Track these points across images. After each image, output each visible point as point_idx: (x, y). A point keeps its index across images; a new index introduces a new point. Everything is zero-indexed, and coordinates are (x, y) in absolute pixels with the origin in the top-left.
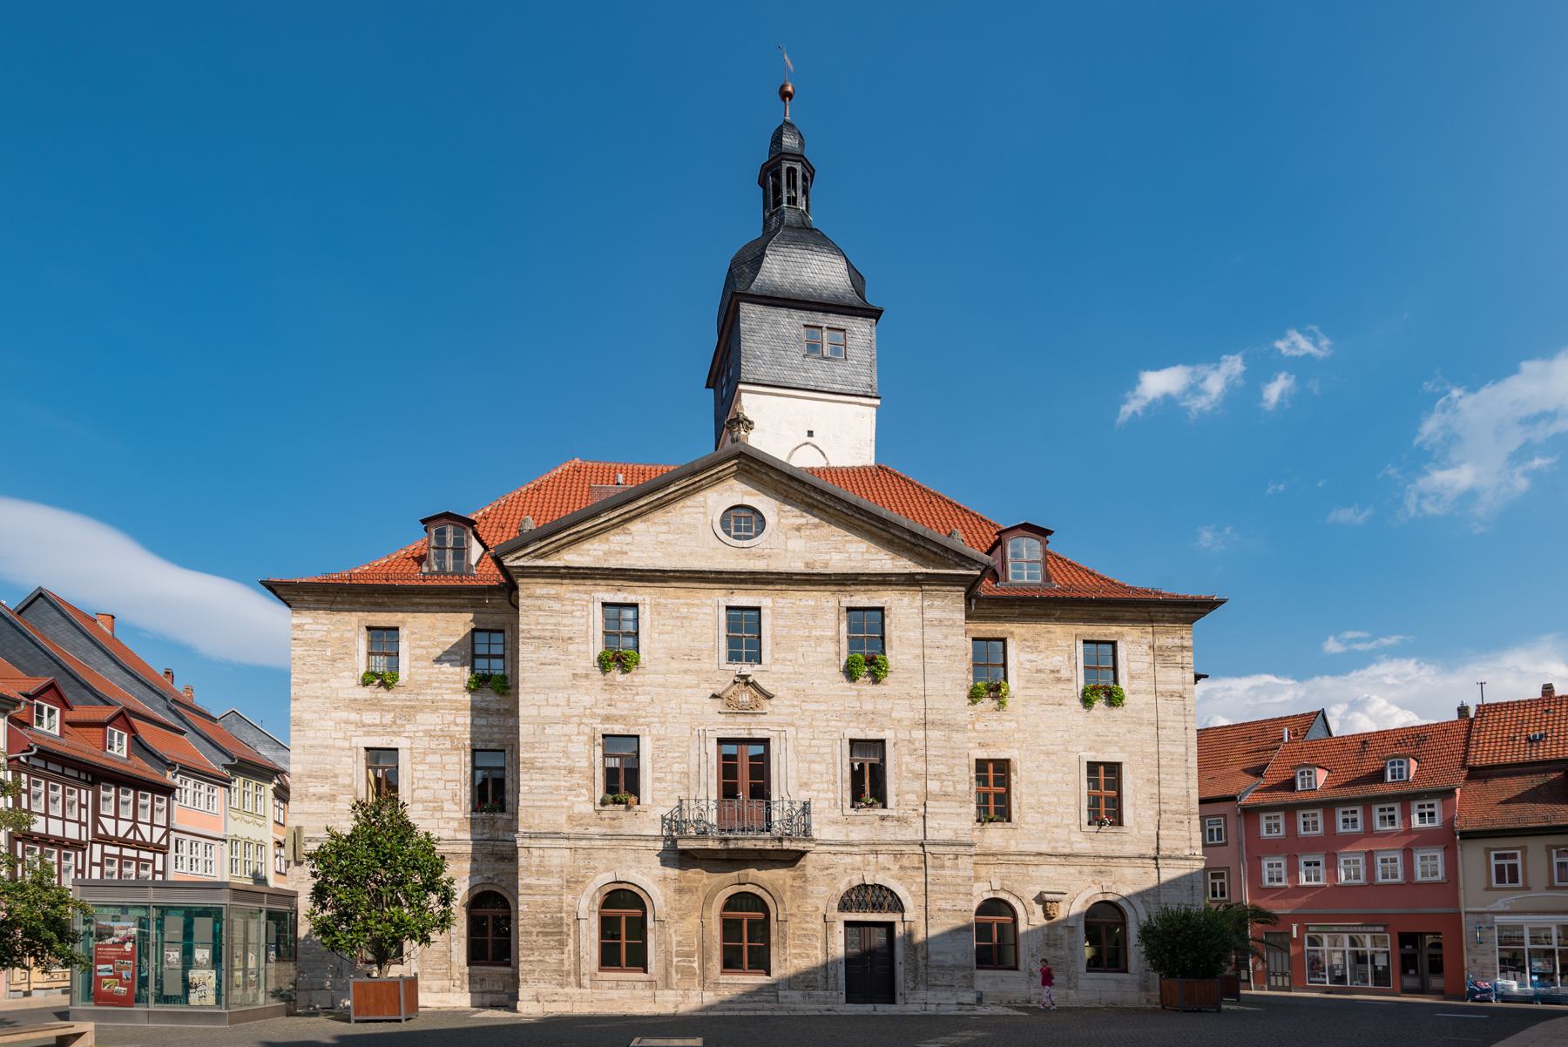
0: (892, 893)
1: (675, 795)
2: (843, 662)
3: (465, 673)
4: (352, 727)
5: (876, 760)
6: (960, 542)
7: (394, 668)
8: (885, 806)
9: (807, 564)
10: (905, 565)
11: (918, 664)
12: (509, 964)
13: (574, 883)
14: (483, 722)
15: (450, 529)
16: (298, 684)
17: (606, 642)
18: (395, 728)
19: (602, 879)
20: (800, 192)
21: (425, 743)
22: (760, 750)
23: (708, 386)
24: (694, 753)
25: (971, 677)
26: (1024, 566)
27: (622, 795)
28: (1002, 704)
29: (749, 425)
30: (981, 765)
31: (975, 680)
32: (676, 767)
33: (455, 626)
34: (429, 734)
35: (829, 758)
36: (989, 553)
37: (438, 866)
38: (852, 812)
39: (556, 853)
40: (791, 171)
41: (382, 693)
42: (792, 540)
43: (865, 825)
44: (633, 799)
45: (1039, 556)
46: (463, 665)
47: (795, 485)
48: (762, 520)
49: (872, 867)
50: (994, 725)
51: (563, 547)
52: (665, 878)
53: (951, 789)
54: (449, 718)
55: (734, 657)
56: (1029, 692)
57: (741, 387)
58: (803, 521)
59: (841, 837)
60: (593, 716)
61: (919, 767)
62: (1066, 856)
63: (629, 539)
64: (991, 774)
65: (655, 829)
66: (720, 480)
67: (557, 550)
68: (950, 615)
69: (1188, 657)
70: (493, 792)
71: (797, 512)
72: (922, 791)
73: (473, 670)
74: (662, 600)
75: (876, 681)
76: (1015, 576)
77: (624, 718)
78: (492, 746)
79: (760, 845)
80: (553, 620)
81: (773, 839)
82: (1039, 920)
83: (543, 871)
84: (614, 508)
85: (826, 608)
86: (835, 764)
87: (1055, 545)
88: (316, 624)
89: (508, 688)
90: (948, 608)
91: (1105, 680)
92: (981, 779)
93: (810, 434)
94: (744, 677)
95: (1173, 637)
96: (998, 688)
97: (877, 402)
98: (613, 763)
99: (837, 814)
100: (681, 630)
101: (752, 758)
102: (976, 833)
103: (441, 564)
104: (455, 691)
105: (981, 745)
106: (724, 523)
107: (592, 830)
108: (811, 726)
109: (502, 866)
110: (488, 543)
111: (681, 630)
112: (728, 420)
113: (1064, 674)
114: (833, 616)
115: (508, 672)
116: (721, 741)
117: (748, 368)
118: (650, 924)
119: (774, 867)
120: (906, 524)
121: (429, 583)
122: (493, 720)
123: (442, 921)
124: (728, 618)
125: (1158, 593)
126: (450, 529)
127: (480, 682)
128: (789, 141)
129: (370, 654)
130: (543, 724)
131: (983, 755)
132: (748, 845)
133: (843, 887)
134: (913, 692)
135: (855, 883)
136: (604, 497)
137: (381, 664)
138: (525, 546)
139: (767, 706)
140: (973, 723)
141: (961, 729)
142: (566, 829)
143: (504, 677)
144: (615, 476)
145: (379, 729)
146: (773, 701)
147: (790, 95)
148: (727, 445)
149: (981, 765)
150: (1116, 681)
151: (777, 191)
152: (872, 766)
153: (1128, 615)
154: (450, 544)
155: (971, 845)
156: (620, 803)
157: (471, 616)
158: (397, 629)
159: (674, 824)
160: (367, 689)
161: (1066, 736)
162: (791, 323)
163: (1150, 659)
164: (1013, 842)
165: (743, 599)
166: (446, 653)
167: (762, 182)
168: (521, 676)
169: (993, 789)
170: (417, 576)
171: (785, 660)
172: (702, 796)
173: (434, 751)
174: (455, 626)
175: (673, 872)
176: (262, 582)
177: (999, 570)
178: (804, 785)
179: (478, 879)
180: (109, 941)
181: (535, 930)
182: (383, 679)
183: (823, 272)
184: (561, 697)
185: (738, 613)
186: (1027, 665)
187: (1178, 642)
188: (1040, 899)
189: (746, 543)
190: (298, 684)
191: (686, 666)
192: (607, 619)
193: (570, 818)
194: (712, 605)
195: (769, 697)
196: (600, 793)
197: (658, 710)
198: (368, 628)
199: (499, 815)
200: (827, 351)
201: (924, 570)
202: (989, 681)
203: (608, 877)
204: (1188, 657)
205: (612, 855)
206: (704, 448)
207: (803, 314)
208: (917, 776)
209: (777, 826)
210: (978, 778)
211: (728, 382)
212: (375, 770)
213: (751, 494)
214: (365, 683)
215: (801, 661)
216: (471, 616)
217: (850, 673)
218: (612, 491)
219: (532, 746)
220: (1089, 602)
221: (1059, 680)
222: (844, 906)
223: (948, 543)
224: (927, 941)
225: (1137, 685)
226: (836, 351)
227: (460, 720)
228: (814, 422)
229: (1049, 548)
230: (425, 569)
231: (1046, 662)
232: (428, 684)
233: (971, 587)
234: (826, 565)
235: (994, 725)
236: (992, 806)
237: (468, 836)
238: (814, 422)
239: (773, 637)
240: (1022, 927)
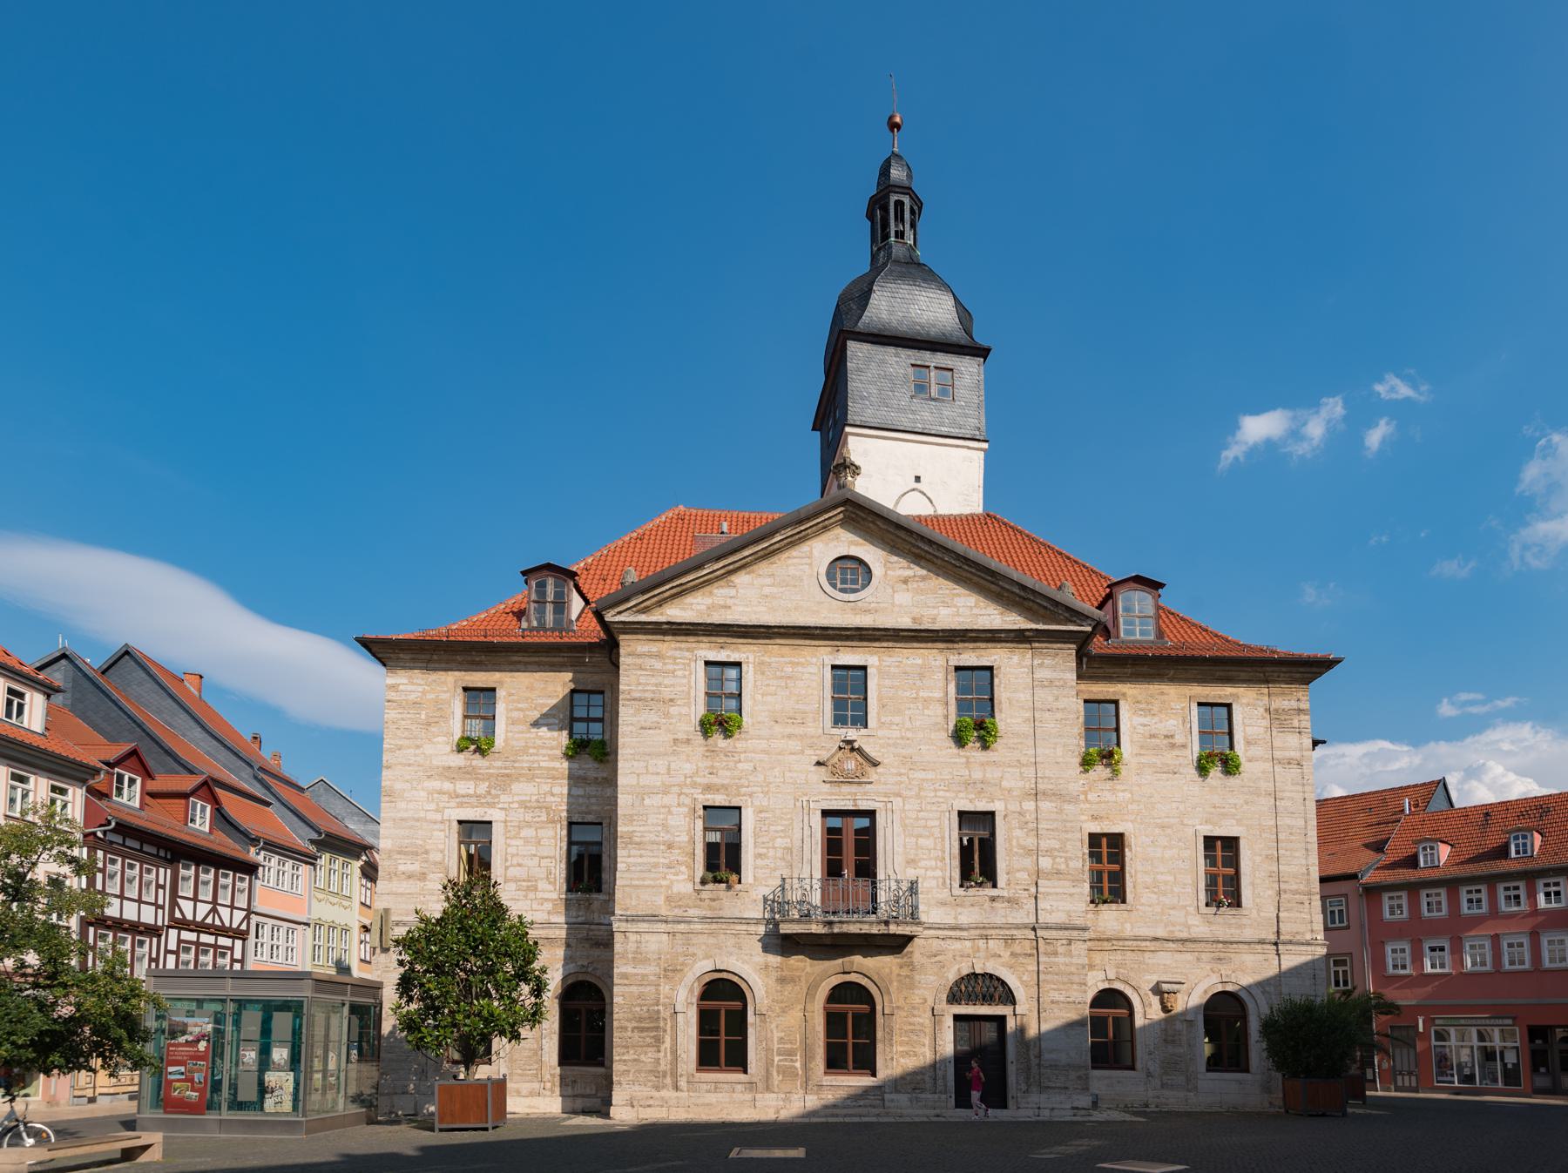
0: (1003, 983)
1: (778, 874)
2: (951, 727)
3: (563, 738)
4: (445, 797)
5: (985, 834)
6: (1070, 595)
7: (490, 732)
8: (995, 886)
9: (914, 620)
10: (1013, 620)
11: (1028, 729)
12: (602, 1064)
13: (671, 972)
14: (580, 792)
15: (550, 582)
16: (391, 751)
17: (708, 704)
18: (489, 799)
19: (700, 968)
20: (907, 226)
21: (518, 815)
22: (864, 822)
23: (814, 429)
24: (797, 826)
25: (1083, 743)
26: (1136, 622)
27: (723, 874)
28: (1115, 773)
29: (855, 470)
30: (1094, 839)
31: (1087, 746)
32: (779, 842)
33: (554, 686)
34: (524, 805)
35: (936, 831)
36: (1100, 607)
37: (530, 954)
38: (961, 892)
39: (654, 938)
40: (899, 204)
41: (478, 761)
42: (902, 593)
43: (975, 907)
44: (734, 877)
45: (1151, 611)
46: (561, 729)
47: (902, 534)
48: (869, 571)
49: (982, 954)
50: (1108, 796)
51: (665, 600)
52: (767, 966)
53: (1063, 867)
54: (546, 788)
55: (839, 720)
56: (1142, 760)
57: (848, 429)
58: (910, 573)
59: (950, 921)
60: (694, 785)
61: (1031, 842)
62: (1184, 941)
63: (732, 592)
64: (1105, 850)
65: (757, 912)
66: (826, 529)
67: (660, 604)
68: (1062, 675)
69: (1305, 721)
70: (589, 870)
71: (904, 563)
72: (1032, 868)
73: (571, 735)
74: (766, 659)
75: (985, 747)
76: (1127, 632)
77: (725, 787)
78: (589, 818)
79: (866, 929)
80: (653, 680)
81: (879, 923)
82: (1156, 1013)
83: (639, 958)
84: (719, 559)
85: (935, 663)
86: (943, 838)
87: (1168, 598)
88: (412, 684)
89: (606, 754)
90: (1059, 665)
91: (1221, 746)
92: (1095, 855)
93: (918, 479)
94: (850, 742)
95: (1291, 698)
96: (1110, 755)
97: (985, 445)
98: (715, 837)
99: (945, 894)
100: (784, 688)
101: (858, 832)
102: (1090, 916)
103: (541, 619)
104: (553, 758)
105: (1094, 818)
106: (830, 575)
107: (691, 912)
108: (918, 796)
109: (596, 952)
110: (589, 596)
111: (784, 688)
112: (834, 465)
113: (1179, 739)
114: (941, 676)
115: (607, 737)
116: (826, 813)
117: (855, 411)
118: (751, 1018)
119: (880, 954)
120: (1015, 576)
121: (529, 640)
122: (591, 790)
123: (534, 1014)
124: (834, 677)
125: (1274, 652)
126: (550, 582)
127: (579, 748)
128: (897, 173)
129: (466, 717)
130: (642, 793)
131: (1097, 829)
132: (853, 929)
133: (952, 977)
134: (1024, 760)
135: (965, 972)
136: (708, 547)
137: (476, 728)
138: (627, 600)
139: (873, 774)
140: (1085, 793)
141: (1074, 800)
142: (664, 912)
143: (603, 743)
144: (720, 525)
145: (473, 800)
146: (880, 769)
147: (898, 126)
148: (833, 491)
149: (1094, 839)
150: (1232, 747)
151: (885, 225)
152: (981, 840)
153: (1243, 675)
154: (550, 597)
155: (1085, 929)
156: (720, 882)
157: (569, 676)
158: (494, 690)
159: (777, 906)
160: (462, 756)
161: (1182, 807)
162: (898, 361)
163: (1266, 723)
164: (1128, 926)
165: (850, 656)
166: (544, 716)
167: (870, 215)
168: (621, 741)
169: (1108, 867)
170: (515, 633)
171: (892, 723)
172: (806, 874)
173: (529, 825)
174: (554, 686)
175: (775, 960)
176: (358, 640)
177: (1110, 627)
178: (911, 862)
179: (572, 968)
180: (182, 1040)
181: (630, 1025)
182: (476, 745)
183: (931, 309)
184: (661, 765)
185: (843, 673)
186: (1141, 729)
187: (1294, 704)
188: (1157, 990)
189: (852, 597)
190: (391, 751)
191: (789, 730)
192: (710, 679)
193: (668, 899)
194: (818, 662)
195: (875, 764)
196: (700, 871)
197: (761, 778)
198: (465, 689)
199: (595, 896)
200: (934, 392)
201: (1034, 626)
202: (1102, 750)
203: (708, 965)
204: (1305, 721)
205: (712, 941)
206: (810, 495)
207: (910, 352)
208: (1028, 852)
209: (884, 909)
210: (1091, 855)
211: (835, 423)
212: (468, 845)
213: (857, 544)
214: (460, 750)
215: (908, 724)
216: (569, 676)
217: (959, 738)
218: (717, 540)
219: (631, 819)
220: (1202, 661)
221: (1173, 746)
222: (953, 998)
223: (1058, 597)
224: (1040, 1037)
225: (1256, 751)
226: (943, 392)
227: (556, 790)
228: (921, 469)
229: (1161, 602)
230: (524, 625)
231: (1160, 726)
232: (525, 750)
233: (1082, 643)
234: (934, 620)
235: (1108, 796)
236: (1106, 885)
237: (562, 919)
238: (921, 469)
239: (880, 699)
240: (1139, 1021)
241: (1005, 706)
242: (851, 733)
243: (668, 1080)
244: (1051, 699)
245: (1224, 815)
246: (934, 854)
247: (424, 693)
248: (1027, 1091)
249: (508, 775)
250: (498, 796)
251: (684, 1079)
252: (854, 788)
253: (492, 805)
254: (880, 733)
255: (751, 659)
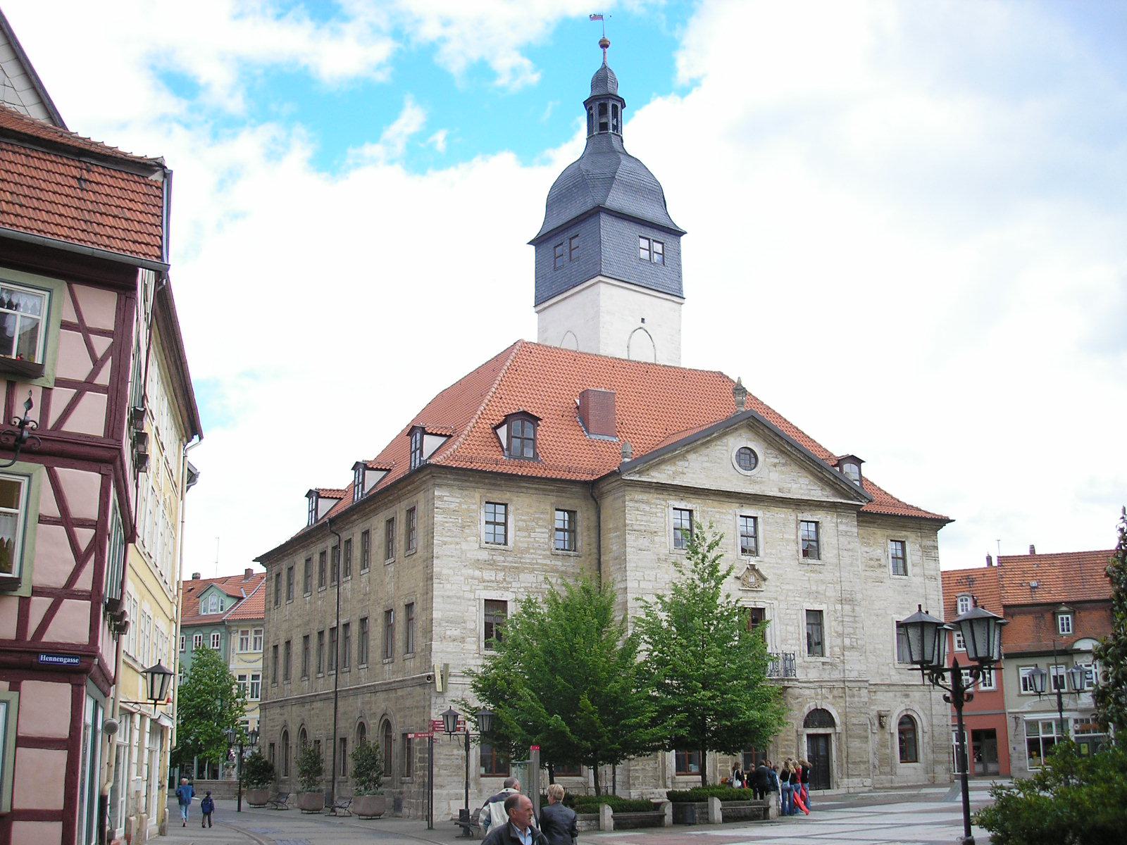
18: (505, 585)
80: (644, 518)
113: (883, 562)
163: (920, 553)
186: (865, 555)
221: (880, 566)
239: (765, 538)
241: (825, 546)
242: (753, 560)
243: (661, 782)
244: (846, 543)
245: (904, 608)
246: (795, 636)
247: (460, 503)
248: (842, 778)
249: (517, 568)
250: (510, 583)
251: (670, 780)
252: (754, 594)
253: (507, 589)
254: (766, 560)
255: (698, 509)
